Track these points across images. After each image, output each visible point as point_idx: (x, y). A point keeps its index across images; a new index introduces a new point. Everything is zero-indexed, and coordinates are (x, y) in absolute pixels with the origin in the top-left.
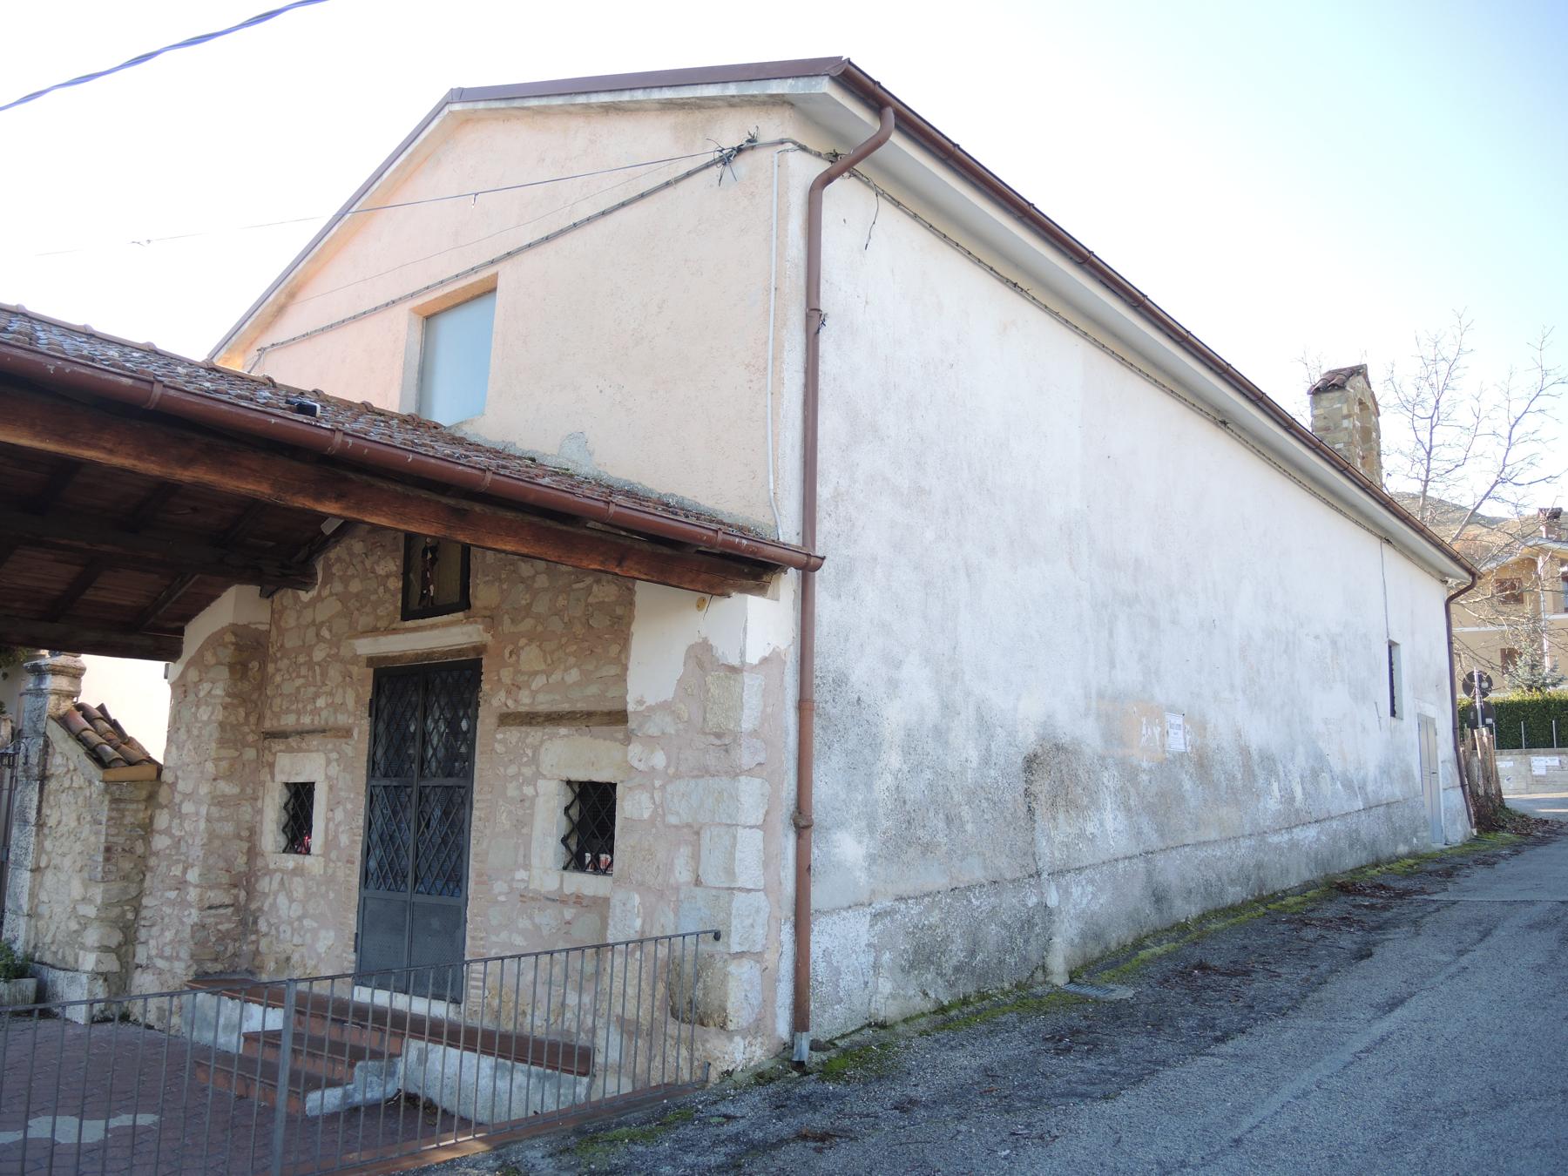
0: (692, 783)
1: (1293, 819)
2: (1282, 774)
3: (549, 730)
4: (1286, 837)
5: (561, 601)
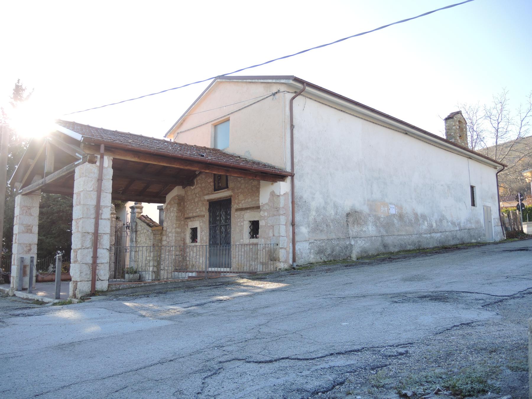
1: (431, 230)
2: (428, 220)
3: (246, 211)
4: (429, 235)
5: (247, 185)
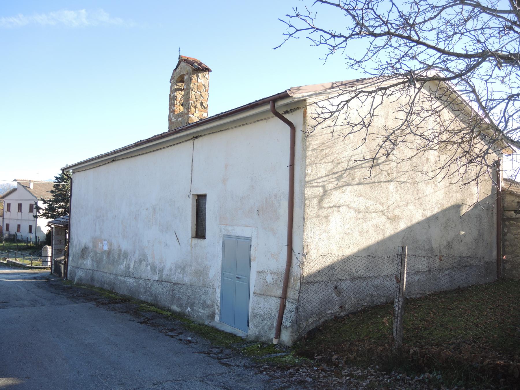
1: (127, 274)
2: (128, 259)
4: (123, 279)
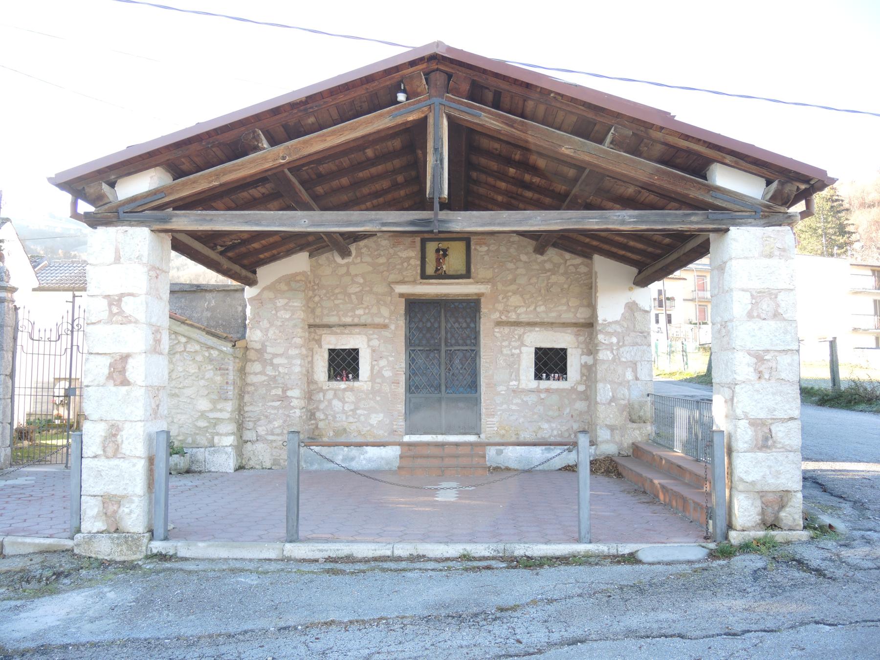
0: (631, 348)
3: (528, 328)
5: (534, 280)
